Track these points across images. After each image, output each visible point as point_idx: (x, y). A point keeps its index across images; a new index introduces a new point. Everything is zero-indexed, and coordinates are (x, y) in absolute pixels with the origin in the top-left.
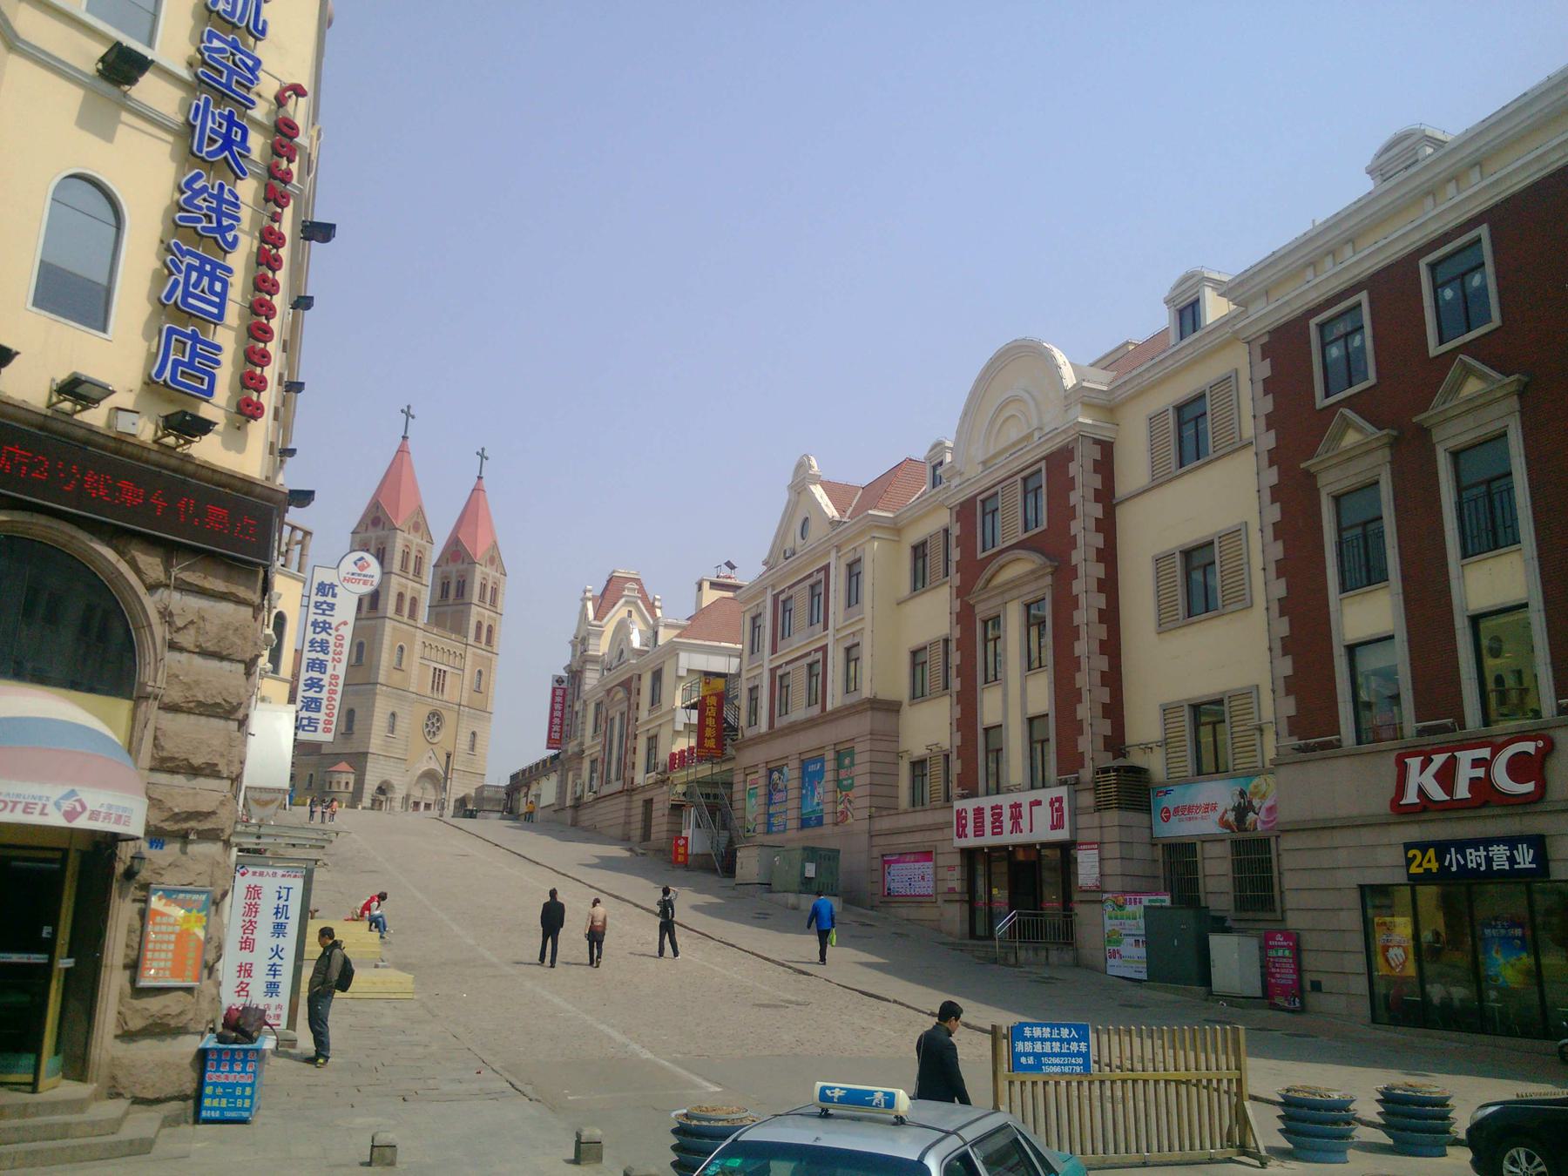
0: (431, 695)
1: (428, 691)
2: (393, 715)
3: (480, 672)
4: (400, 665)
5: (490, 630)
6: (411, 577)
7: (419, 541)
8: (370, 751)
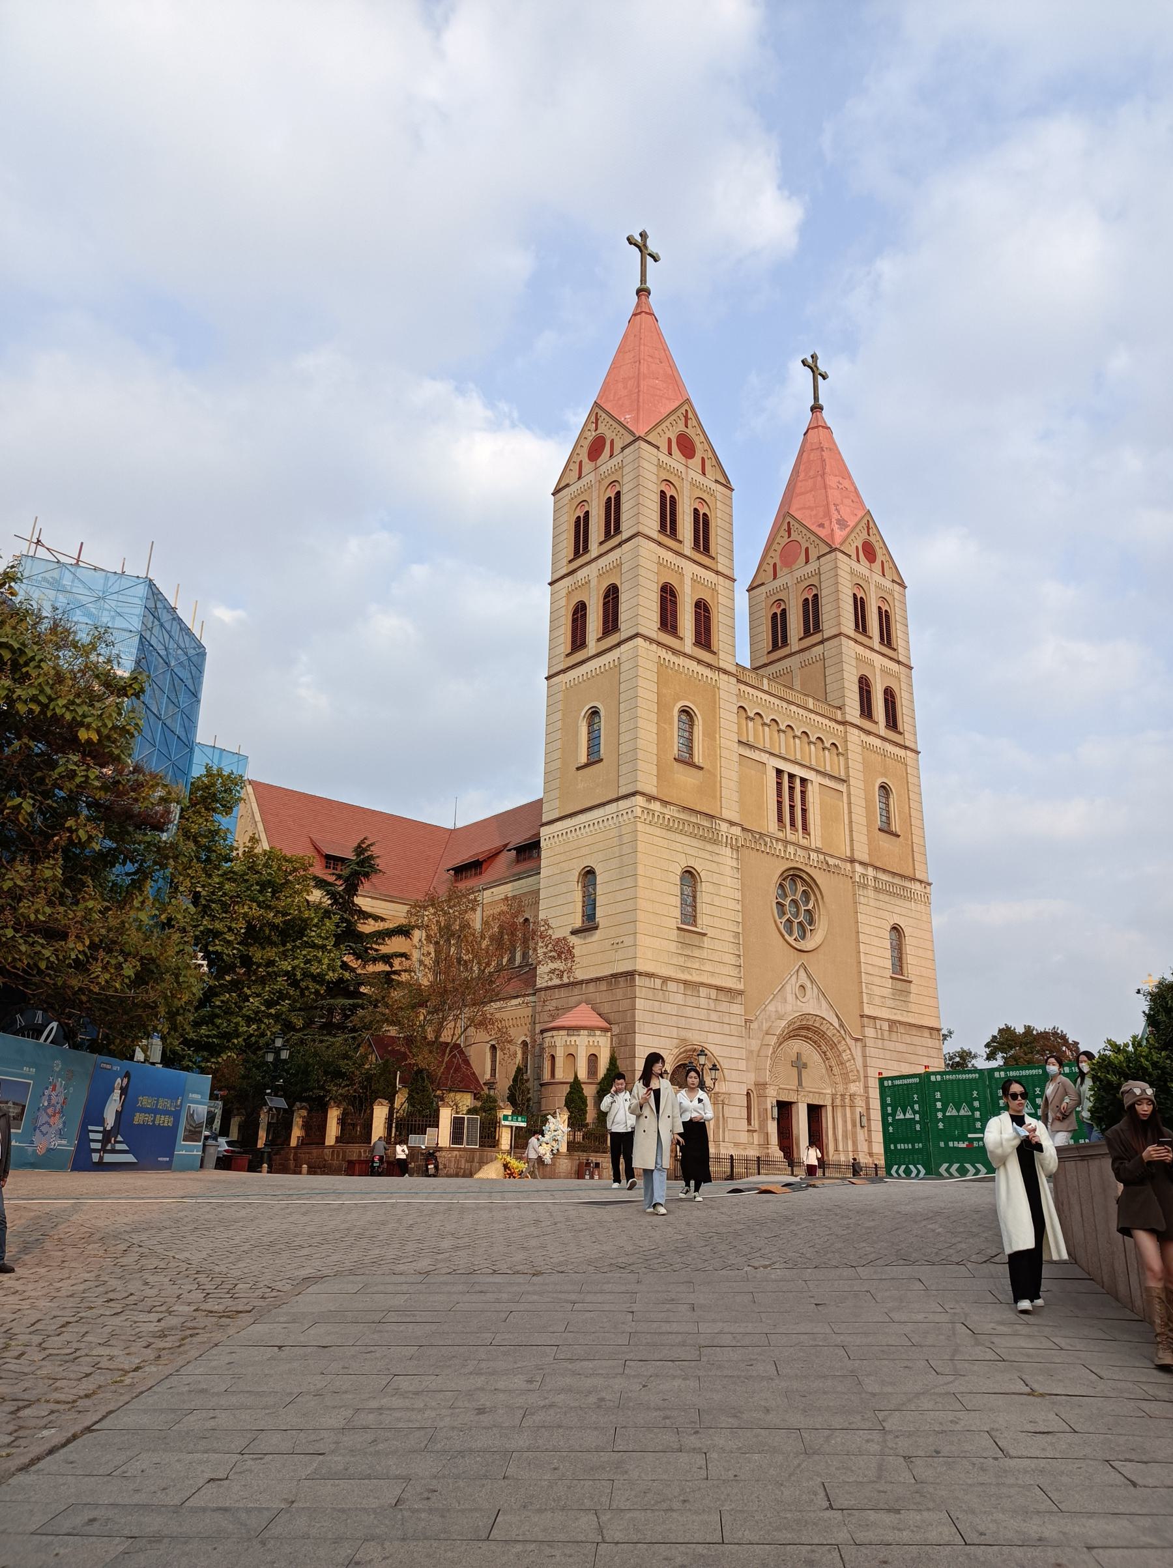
0: (781, 835)
1: (772, 826)
2: (690, 875)
3: (884, 788)
4: (691, 755)
5: (889, 695)
6: (687, 548)
7: (700, 478)
8: (640, 967)
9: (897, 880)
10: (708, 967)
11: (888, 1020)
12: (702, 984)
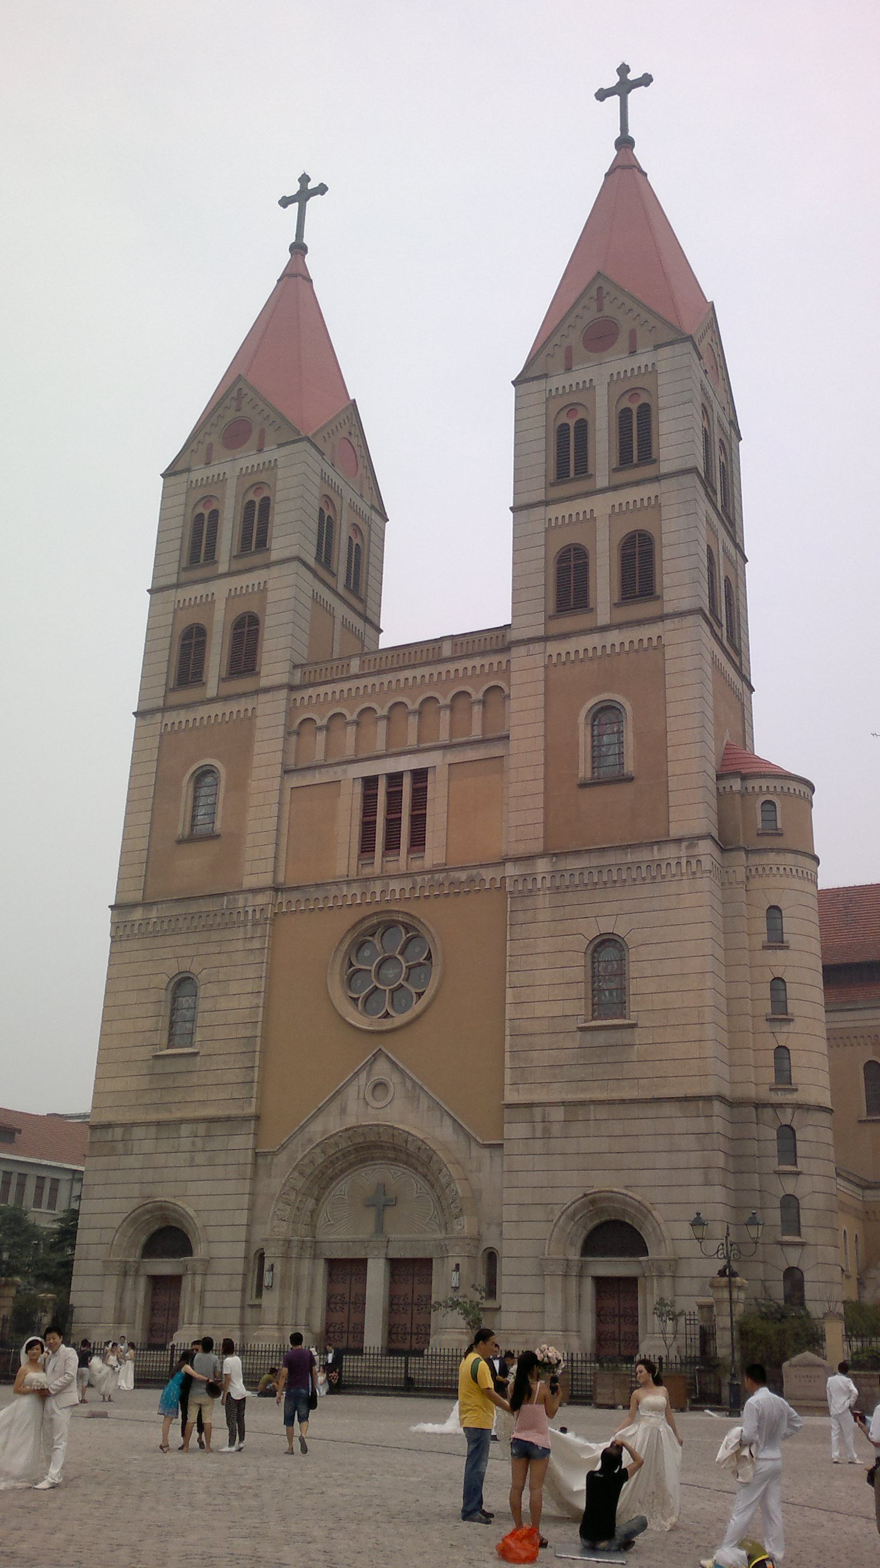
9: (611, 859)
10: (199, 1095)
11: (563, 1103)
12: (182, 1121)
